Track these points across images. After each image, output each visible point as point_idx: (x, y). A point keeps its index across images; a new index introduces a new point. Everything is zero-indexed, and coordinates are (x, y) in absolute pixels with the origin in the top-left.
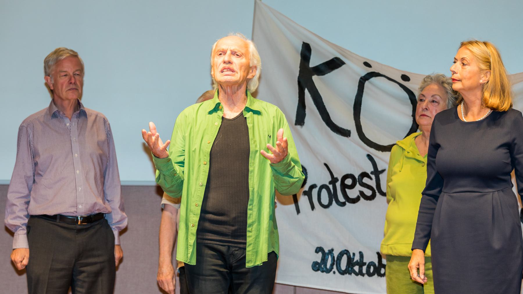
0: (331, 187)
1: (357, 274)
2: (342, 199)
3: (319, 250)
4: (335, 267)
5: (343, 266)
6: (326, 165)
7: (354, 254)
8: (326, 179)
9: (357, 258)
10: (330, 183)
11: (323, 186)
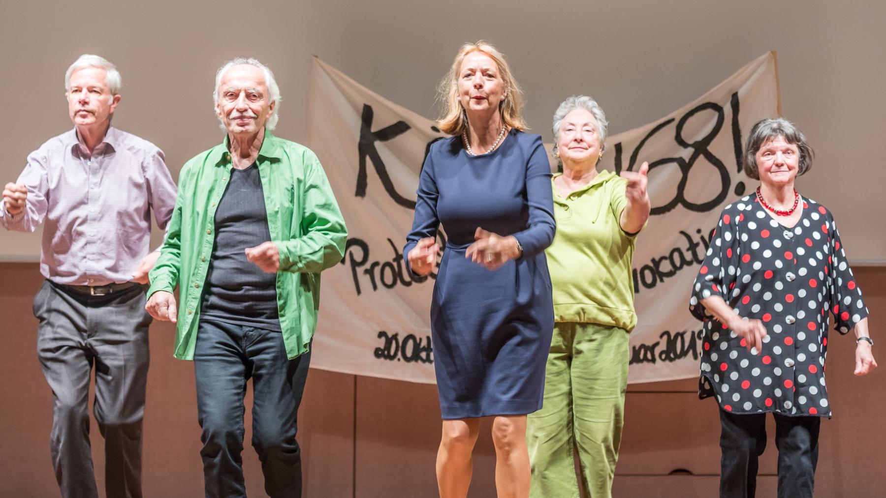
0: (395, 264)
1: (424, 361)
2: (407, 278)
3: (382, 334)
4: (400, 353)
5: (409, 353)
6: (389, 240)
7: (421, 339)
8: (390, 256)
9: (424, 343)
10: (394, 260)
11: (388, 264)
